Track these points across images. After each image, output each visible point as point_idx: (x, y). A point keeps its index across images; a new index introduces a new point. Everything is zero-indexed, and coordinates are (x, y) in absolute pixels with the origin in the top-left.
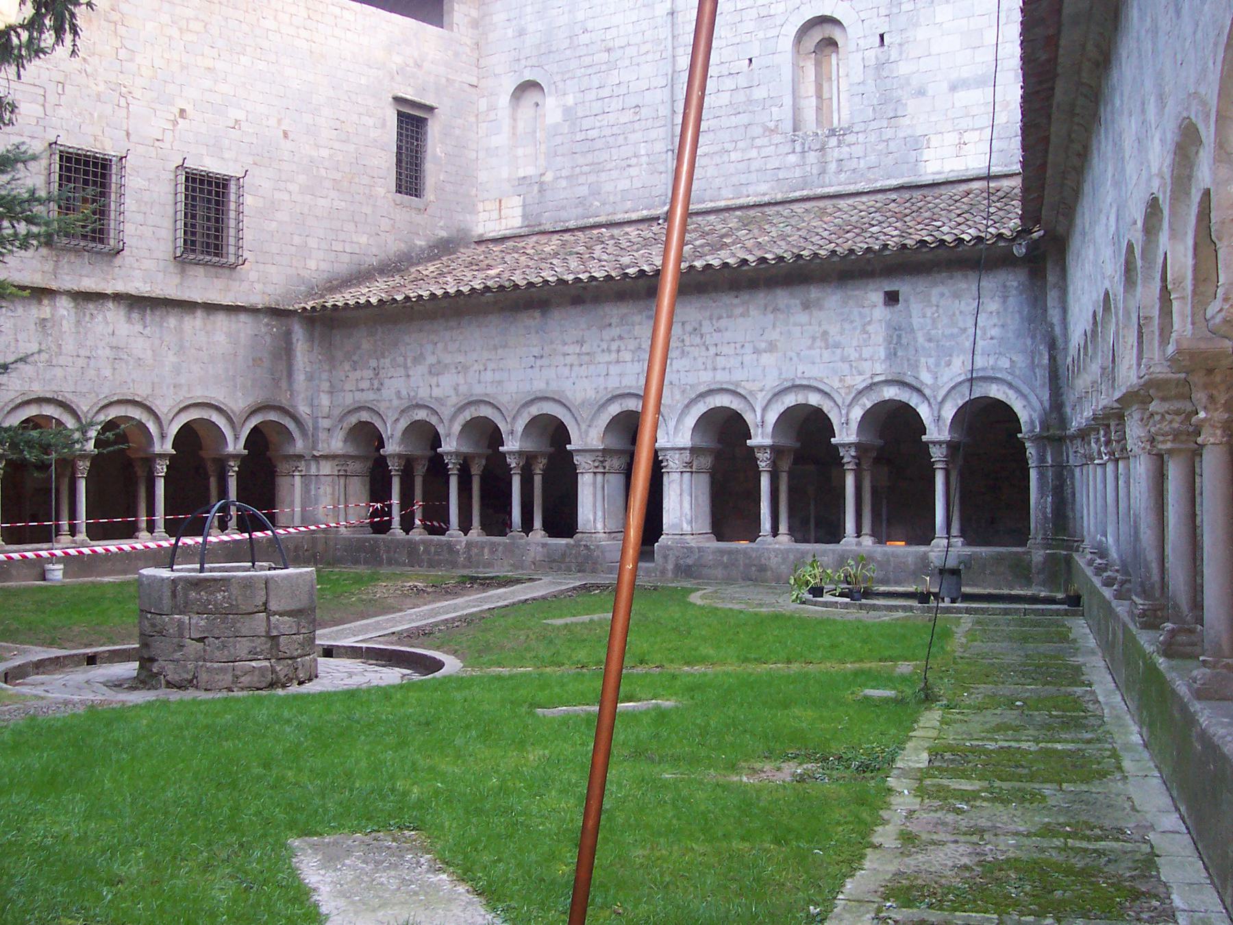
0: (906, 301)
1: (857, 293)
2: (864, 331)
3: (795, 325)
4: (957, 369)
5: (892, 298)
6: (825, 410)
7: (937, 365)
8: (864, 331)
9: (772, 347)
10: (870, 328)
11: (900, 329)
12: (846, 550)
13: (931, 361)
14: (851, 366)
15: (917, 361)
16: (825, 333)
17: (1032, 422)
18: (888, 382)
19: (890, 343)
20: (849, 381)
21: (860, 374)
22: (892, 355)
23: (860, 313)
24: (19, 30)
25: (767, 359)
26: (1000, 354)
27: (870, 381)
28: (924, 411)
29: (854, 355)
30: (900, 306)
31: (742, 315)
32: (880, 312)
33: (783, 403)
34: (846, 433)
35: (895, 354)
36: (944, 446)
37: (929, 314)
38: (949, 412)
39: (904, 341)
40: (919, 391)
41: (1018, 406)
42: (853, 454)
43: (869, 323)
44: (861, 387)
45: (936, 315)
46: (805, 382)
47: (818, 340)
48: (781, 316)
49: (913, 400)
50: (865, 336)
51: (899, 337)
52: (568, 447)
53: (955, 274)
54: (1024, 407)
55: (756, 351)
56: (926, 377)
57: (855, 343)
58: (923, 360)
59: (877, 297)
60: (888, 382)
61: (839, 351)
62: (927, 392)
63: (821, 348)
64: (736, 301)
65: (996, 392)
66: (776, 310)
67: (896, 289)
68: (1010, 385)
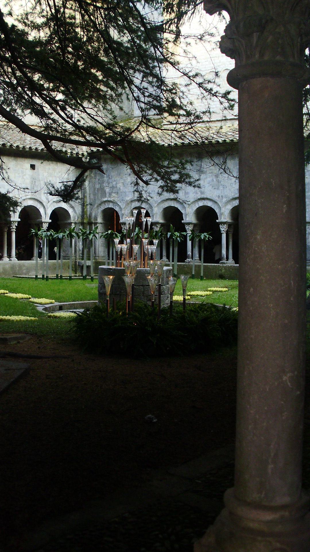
0: (38, 169)
1: (21, 163)
2: (23, 178)
5: (33, 167)
8: (23, 178)
10: (25, 177)
12: (15, 263)
17: (74, 217)
18: (31, 199)
24: (235, 40)
32: (29, 171)
36: (48, 224)
37: (45, 175)
38: (49, 212)
39: (37, 184)
40: (41, 203)
42: (17, 225)
43: (25, 175)
45: (47, 176)
51: (35, 182)
52: (183, 221)
53: (53, 162)
54: (72, 212)
60: (31, 199)
62: (44, 204)
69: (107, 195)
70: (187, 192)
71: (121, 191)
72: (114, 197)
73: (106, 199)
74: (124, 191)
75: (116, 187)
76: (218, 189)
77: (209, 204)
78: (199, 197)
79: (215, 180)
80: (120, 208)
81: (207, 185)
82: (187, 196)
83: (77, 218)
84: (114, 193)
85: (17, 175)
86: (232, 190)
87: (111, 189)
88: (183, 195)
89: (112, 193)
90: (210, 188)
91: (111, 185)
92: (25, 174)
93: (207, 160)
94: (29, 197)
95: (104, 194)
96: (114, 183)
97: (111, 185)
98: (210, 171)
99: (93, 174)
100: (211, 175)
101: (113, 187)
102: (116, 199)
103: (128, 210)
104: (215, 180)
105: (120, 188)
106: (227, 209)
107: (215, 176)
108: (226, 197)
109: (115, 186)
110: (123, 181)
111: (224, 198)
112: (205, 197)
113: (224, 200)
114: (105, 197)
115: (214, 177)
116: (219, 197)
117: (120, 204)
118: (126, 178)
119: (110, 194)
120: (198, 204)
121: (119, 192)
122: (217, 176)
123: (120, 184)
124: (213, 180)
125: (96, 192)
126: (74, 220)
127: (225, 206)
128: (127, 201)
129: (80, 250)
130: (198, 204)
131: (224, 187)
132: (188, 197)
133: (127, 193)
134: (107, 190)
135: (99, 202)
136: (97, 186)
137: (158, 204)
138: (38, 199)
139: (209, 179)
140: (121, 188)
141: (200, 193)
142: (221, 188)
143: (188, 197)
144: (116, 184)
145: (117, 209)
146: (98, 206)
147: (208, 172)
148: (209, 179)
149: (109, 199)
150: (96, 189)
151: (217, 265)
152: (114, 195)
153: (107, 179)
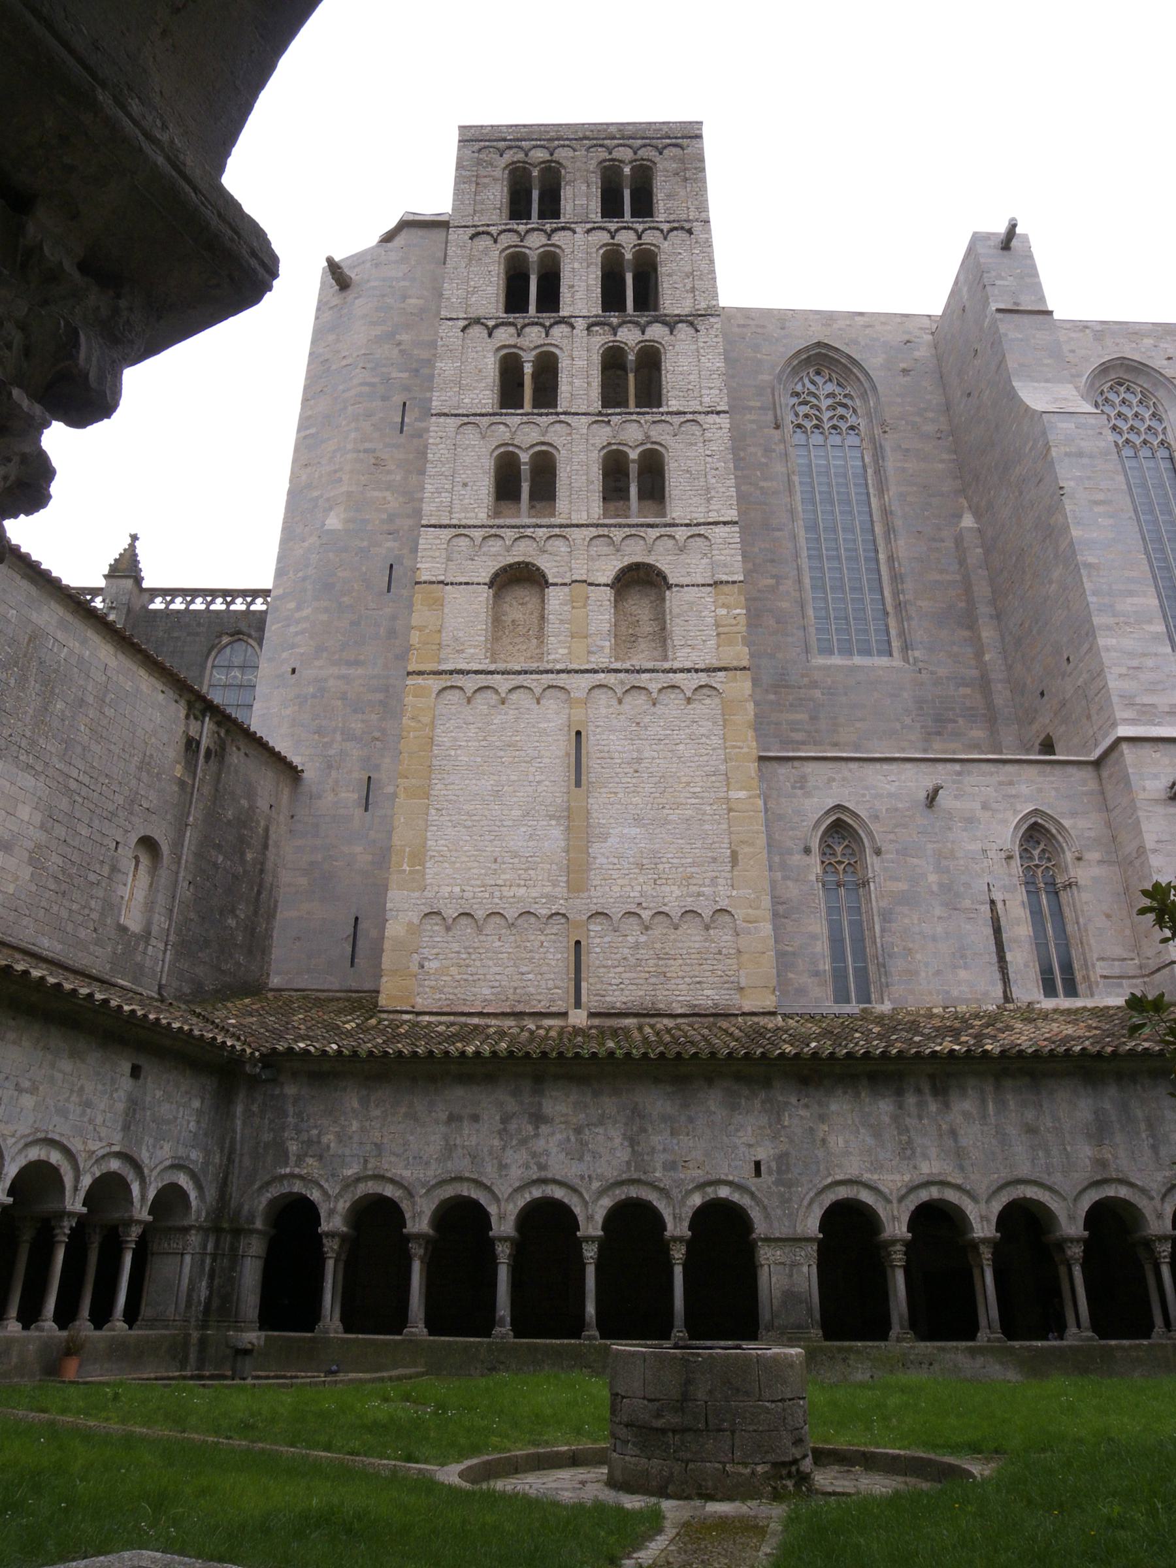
0: (146, 1078)
3: (60, 1071)
4: (167, 1152)
5: (136, 1072)
6: (62, 1171)
7: (154, 1146)
9: (33, 1090)
10: (115, 1095)
11: (136, 1104)
13: (151, 1141)
14: (95, 1129)
15: (142, 1138)
16: (82, 1089)
17: (199, 1212)
18: (118, 1155)
19: (127, 1115)
20: (93, 1146)
21: (101, 1140)
22: (126, 1128)
23: (112, 1079)
25: (28, 1101)
26: (193, 1147)
27: (107, 1150)
28: (135, 1188)
29: (99, 1120)
30: (141, 1081)
31: (14, 1043)
33: (26, 1156)
34: (333, 1222)
35: (129, 1128)
37: (157, 1097)
39: (137, 1116)
41: (193, 1195)
43: (117, 1090)
44: (101, 1153)
46: (57, 1138)
47: (75, 1095)
48: (50, 1057)
49: (131, 1176)
50: (111, 1102)
51: (134, 1110)
55: (19, 1089)
56: (144, 1156)
57: (102, 1106)
58: (146, 1138)
59: (126, 1067)
60: (118, 1155)
61: (89, 1111)
62: (146, 1171)
63: (75, 1104)
64: (12, 1023)
65: (183, 1180)
66: (46, 1048)
67: (140, 1063)
68: (194, 1176)
69: (293, 1159)
70: (504, 1163)
71: (332, 1152)
72: (311, 1166)
73: (288, 1170)
74: (340, 1152)
75: (319, 1142)
76: (581, 1159)
77: (558, 1193)
78: (535, 1177)
79: (573, 1139)
80: (325, 1193)
81: (554, 1150)
82: (504, 1173)
83: (204, 1214)
84: (311, 1156)
85: (100, 1087)
86: (614, 1163)
87: (304, 1146)
88: (495, 1170)
89: (306, 1155)
90: (562, 1156)
91: (304, 1137)
92: (117, 1086)
93: (554, 1094)
94: (116, 1148)
95: (283, 1156)
96: (315, 1132)
97: (304, 1137)
98: (563, 1119)
99: (256, 1105)
100: (563, 1126)
101: (310, 1142)
102: (316, 1173)
103: (345, 1202)
104: (573, 1139)
105: (328, 1147)
106: (602, 1206)
107: (575, 1129)
108: (600, 1177)
109: (315, 1139)
110: (337, 1129)
111: (594, 1181)
112: (550, 1176)
113: (596, 1185)
114: (286, 1164)
115: (571, 1133)
116: (582, 1177)
117: (326, 1186)
118: (347, 1123)
119: (300, 1159)
120: (530, 1193)
121: (325, 1155)
122: (578, 1131)
123: (329, 1137)
124: (568, 1140)
125: (261, 1151)
126: (197, 1220)
127: (598, 1199)
128: (345, 1178)
129: (199, 1302)
130: (530, 1193)
131: (596, 1155)
132: (506, 1175)
133: (348, 1159)
134: (293, 1147)
135: (267, 1178)
136: (267, 1137)
137: (428, 1191)
138: (136, 1156)
139: (558, 1136)
140: (332, 1145)
141: (535, 1168)
142: (588, 1158)
143: (506, 1175)
144: (319, 1135)
145: (315, 1195)
146: (261, 1188)
147: (557, 1121)
148: (558, 1136)
149: (297, 1171)
150: (262, 1145)
151: (578, 1342)
152: (310, 1161)
153: (296, 1121)
